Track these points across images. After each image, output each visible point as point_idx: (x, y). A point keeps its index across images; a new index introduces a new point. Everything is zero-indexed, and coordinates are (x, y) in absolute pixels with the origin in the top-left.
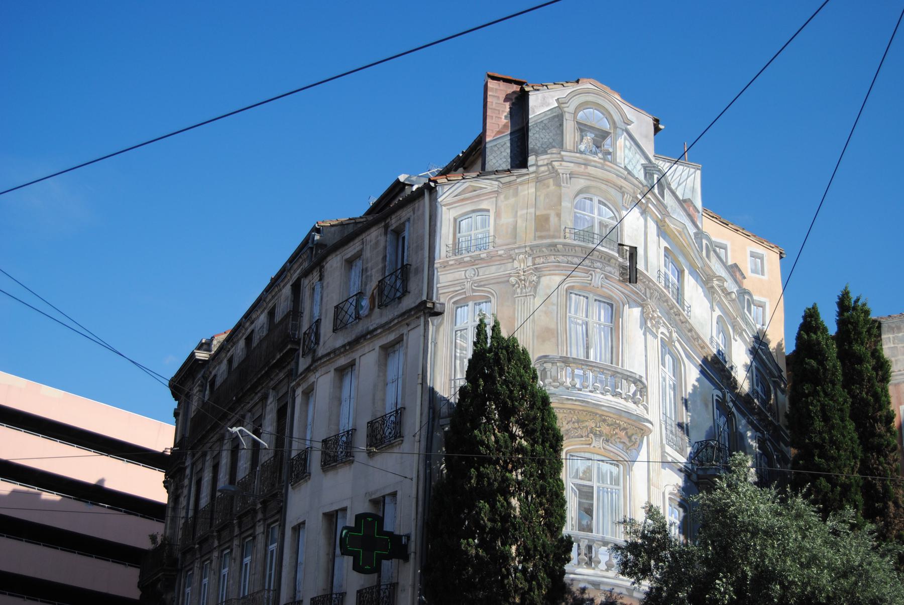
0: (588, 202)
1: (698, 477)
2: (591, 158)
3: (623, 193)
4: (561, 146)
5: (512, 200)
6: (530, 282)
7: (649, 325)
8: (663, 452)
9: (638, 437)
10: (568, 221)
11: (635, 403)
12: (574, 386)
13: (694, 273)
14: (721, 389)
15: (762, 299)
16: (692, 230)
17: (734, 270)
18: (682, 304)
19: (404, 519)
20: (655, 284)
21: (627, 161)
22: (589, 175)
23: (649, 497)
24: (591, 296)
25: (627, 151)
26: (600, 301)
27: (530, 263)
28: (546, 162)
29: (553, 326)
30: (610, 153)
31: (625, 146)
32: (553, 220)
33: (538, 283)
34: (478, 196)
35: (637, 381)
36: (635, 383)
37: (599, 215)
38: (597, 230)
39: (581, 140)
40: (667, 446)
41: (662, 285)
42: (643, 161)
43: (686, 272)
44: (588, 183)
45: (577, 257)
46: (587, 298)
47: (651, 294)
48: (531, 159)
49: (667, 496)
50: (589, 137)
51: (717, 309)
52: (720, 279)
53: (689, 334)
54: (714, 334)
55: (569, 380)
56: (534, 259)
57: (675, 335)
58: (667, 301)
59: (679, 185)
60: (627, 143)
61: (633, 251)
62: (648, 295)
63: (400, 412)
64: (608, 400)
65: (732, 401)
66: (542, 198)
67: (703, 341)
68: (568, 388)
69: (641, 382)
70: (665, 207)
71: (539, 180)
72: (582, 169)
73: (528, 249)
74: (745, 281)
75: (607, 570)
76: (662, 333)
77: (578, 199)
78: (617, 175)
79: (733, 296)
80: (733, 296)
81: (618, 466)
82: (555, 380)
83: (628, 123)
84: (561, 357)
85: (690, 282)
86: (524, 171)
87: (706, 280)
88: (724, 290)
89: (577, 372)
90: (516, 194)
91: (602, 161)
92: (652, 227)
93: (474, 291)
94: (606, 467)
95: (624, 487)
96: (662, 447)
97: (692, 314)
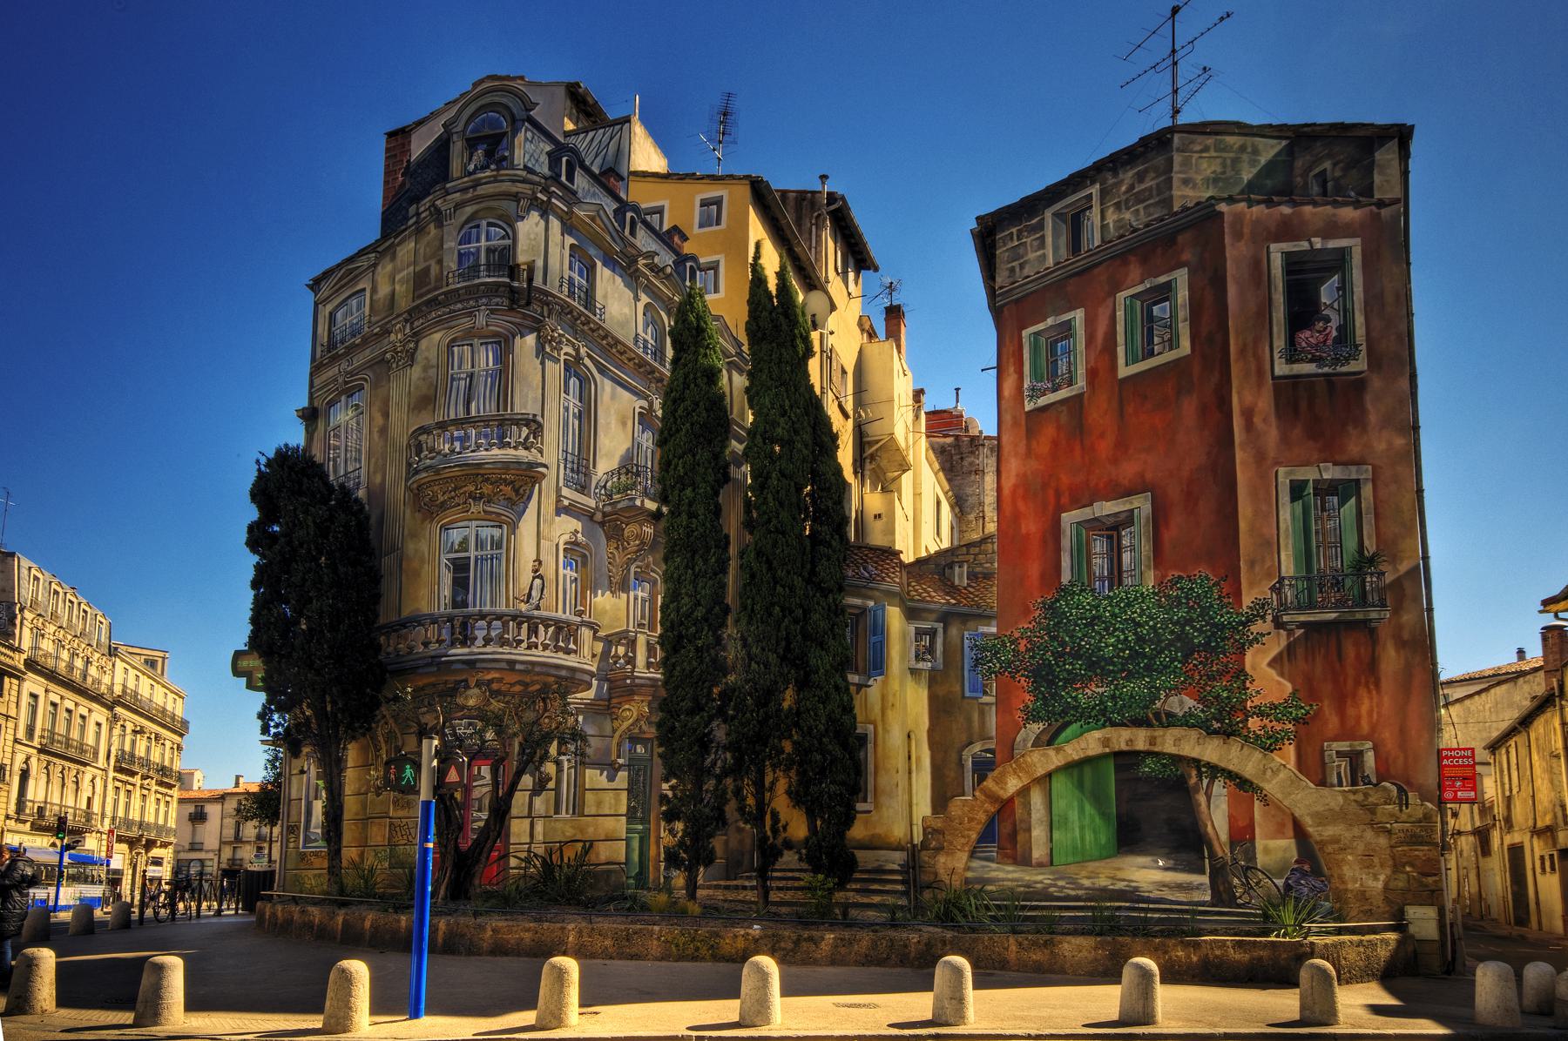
1: (605, 515)
9: (528, 488)
12: (452, 451)
13: (609, 262)
14: (646, 398)
17: (671, 237)
20: (554, 296)
24: (476, 341)
43: (599, 264)
44: (475, 207)
49: (561, 547)
54: (640, 330)
57: (583, 351)
58: (571, 312)
60: (529, 135)
61: (531, 269)
67: (624, 345)
69: (535, 421)
78: (513, 181)
82: (432, 450)
85: (603, 274)
89: (456, 434)
92: (555, 224)
94: (486, 533)
96: (558, 490)
97: (607, 316)
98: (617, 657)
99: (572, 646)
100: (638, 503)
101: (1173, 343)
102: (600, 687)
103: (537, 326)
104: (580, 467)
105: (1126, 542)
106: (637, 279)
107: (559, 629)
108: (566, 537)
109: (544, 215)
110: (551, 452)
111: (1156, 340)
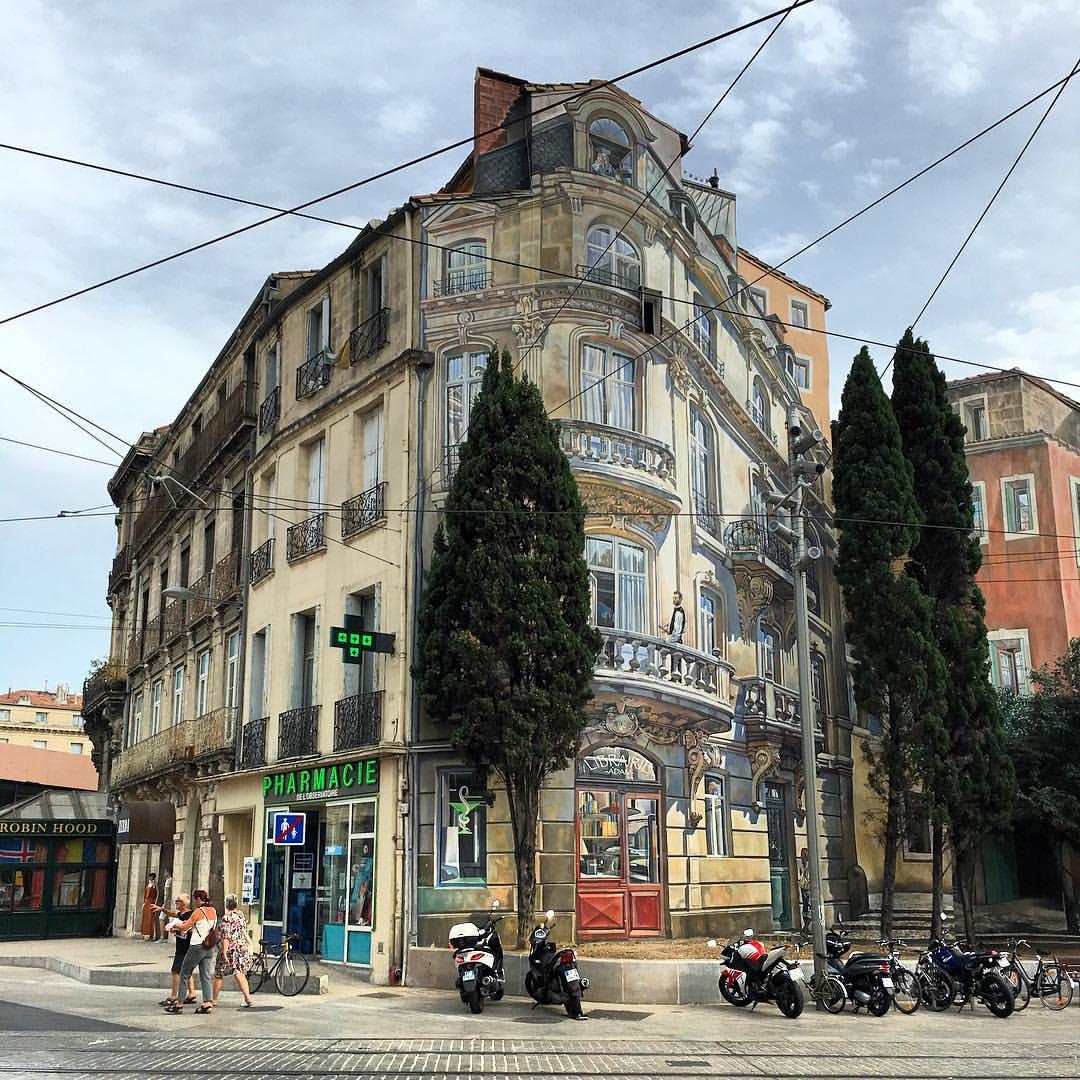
0: (603, 234)
2: (607, 180)
3: (645, 225)
4: (571, 163)
5: (513, 229)
6: (537, 331)
7: (676, 385)
8: (694, 534)
10: (580, 257)
11: (660, 477)
12: (590, 456)
15: (806, 358)
16: (726, 273)
17: (773, 321)
18: (714, 362)
19: (394, 616)
21: (649, 187)
22: (605, 202)
23: (678, 587)
24: (608, 349)
25: (649, 172)
26: (619, 355)
27: (536, 308)
28: (553, 183)
29: (565, 384)
30: (629, 176)
31: (648, 167)
32: (563, 255)
33: (546, 330)
34: (471, 222)
35: (663, 451)
36: (660, 453)
37: (620, 251)
38: (614, 270)
39: (595, 158)
40: (698, 527)
41: (691, 338)
42: (669, 187)
43: (719, 323)
45: (592, 301)
46: (604, 351)
47: (679, 348)
48: (536, 179)
49: (699, 585)
50: (605, 154)
51: (753, 366)
52: (758, 332)
53: (722, 397)
54: (751, 398)
55: (584, 449)
56: (540, 303)
57: (706, 398)
58: (696, 357)
59: (710, 218)
62: (675, 350)
63: (381, 488)
64: (630, 473)
65: (771, 475)
66: (549, 227)
67: (739, 407)
68: (583, 459)
69: (668, 452)
70: (695, 244)
71: (545, 206)
72: (596, 193)
73: (533, 290)
74: (786, 335)
75: (632, 671)
76: (691, 395)
77: (592, 229)
79: (773, 353)
80: (773, 353)
81: (642, 550)
83: (651, 138)
84: (576, 422)
85: (723, 334)
86: (527, 193)
87: (742, 336)
88: (762, 345)
90: (517, 222)
91: (619, 184)
92: (679, 267)
93: (469, 339)
94: (628, 552)
95: (650, 575)
96: (693, 529)
98: (750, 701)
99: (711, 685)
100: (760, 559)
101: (1031, 528)
102: (738, 730)
103: (668, 361)
104: (710, 513)
105: (1018, 662)
106: (749, 349)
107: (700, 666)
108: (701, 577)
109: (669, 250)
110: (683, 487)
111: (1022, 520)
